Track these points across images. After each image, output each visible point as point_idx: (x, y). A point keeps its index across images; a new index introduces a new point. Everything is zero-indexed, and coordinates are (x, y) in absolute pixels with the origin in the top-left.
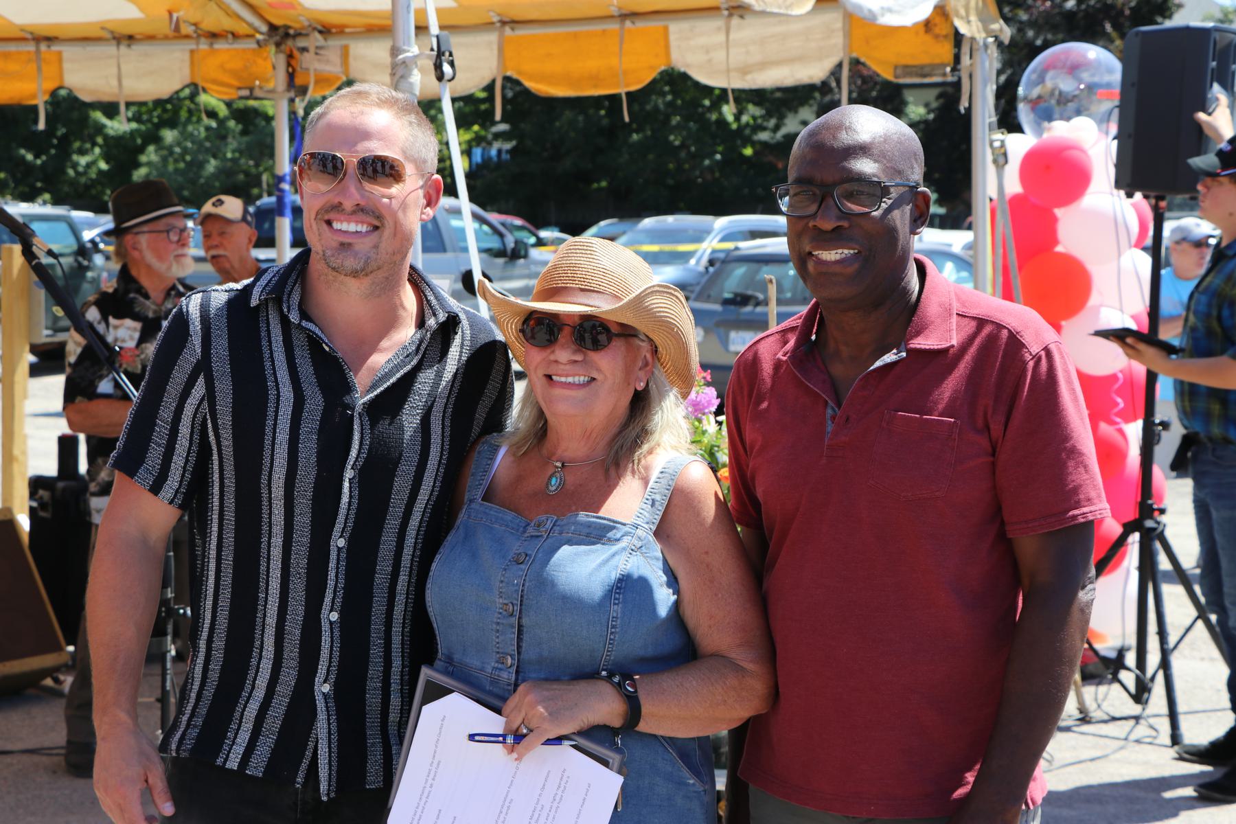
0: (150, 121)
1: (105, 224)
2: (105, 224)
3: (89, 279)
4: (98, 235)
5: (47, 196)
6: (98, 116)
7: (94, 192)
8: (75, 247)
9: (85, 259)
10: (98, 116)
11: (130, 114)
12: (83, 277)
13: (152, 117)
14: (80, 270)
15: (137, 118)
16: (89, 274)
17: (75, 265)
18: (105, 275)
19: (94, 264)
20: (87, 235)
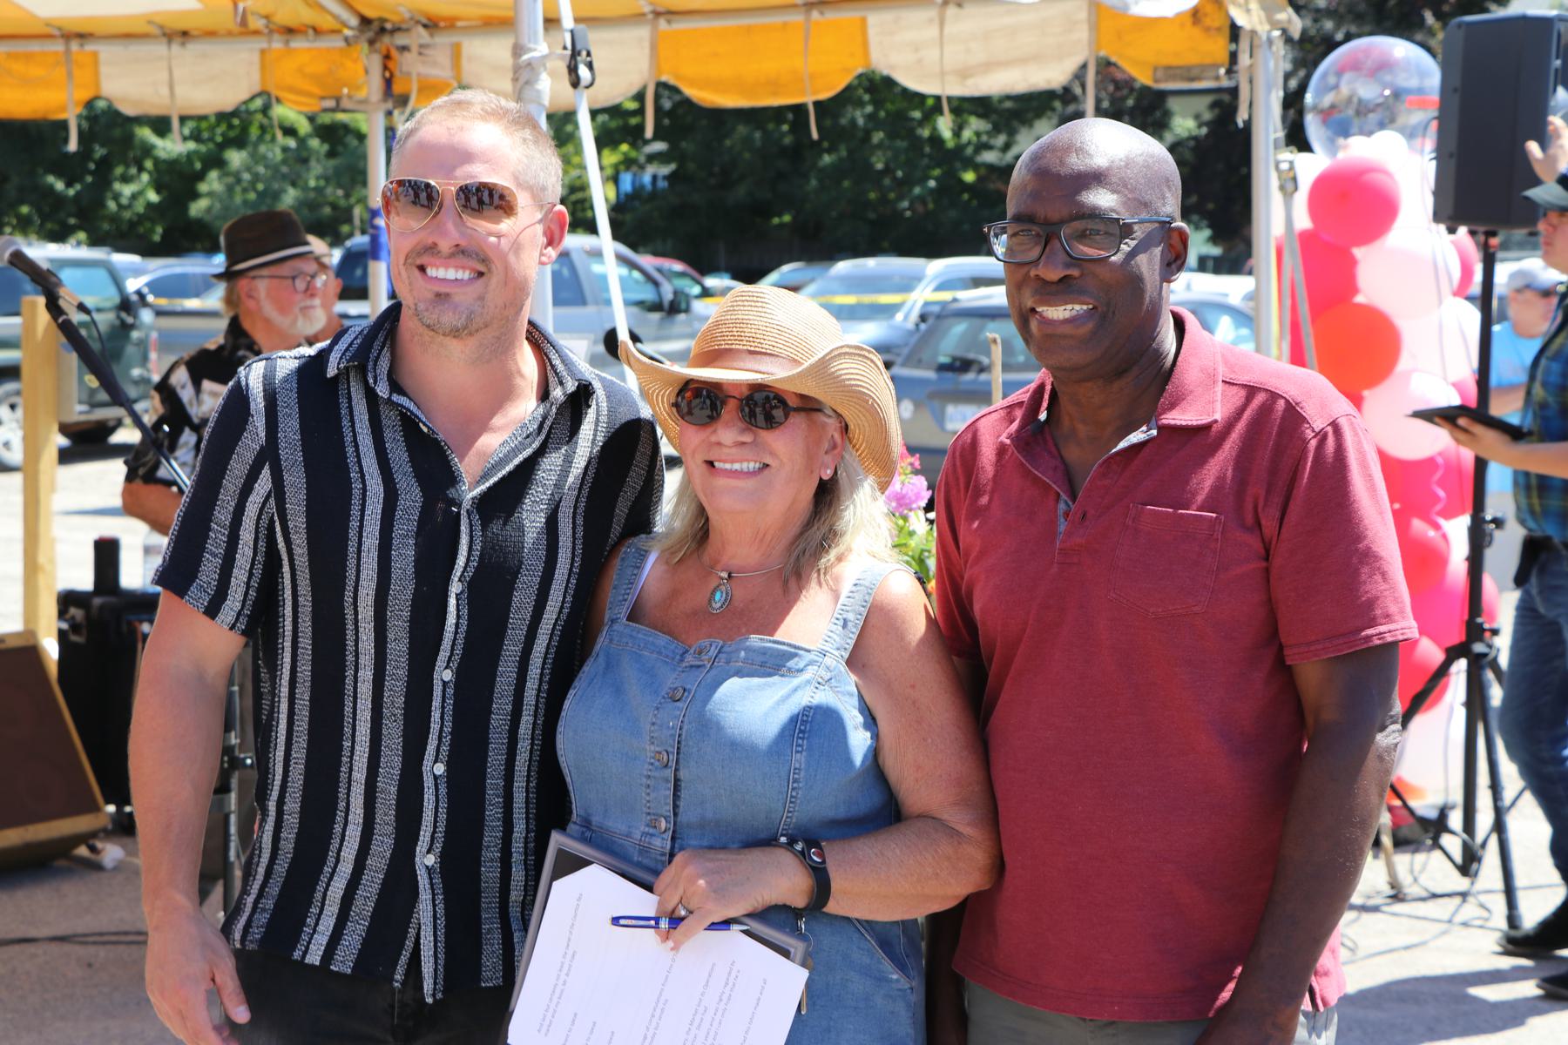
0: (211, 139)
1: (155, 270)
2: (155, 270)
3: (135, 342)
4: (148, 285)
5: (82, 235)
6: (145, 133)
7: (141, 230)
8: (117, 300)
9: (129, 314)
10: (145, 133)
11: (186, 131)
12: (127, 337)
13: (214, 135)
14: (125, 328)
15: (196, 136)
16: (135, 335)
17: (117, 322)
18: (154, 335)
19: (142, 324)
20: (132, 285)
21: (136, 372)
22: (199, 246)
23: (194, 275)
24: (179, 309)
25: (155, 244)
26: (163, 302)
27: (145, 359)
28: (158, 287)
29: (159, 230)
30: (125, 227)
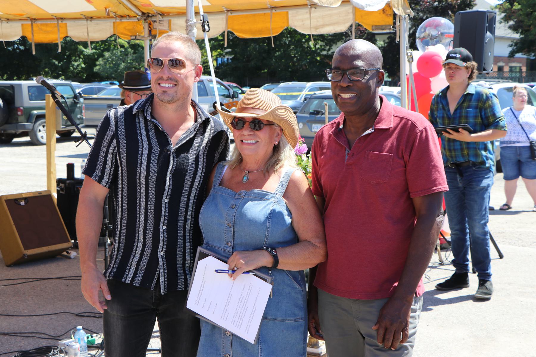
0: (100, 49)
1: (83, 87)
2: (83, 87)
3: (79, 107)
4: (81, 91)
5: (63, 77)
6: (81, 47)
7: (80, 75)
8: (73, 95)
9: (76, 100)
10: (81, 47)
11: (93, 47)
12: (76, 106)
13: (101, 48)
14: (75, 104)
15: (95, 48)
16: (78, 105)
17: (73, 102)
18: (84, 105)
19: (80, 101)
20: (77, 91)
21: (79, 116)
22: (96, 80)
23: (95, 87)
24: (91, 98)
26: (86, 96)
27: (81, 112)
28: (84, 91)
29: (85, 75)
30: (75, 74)
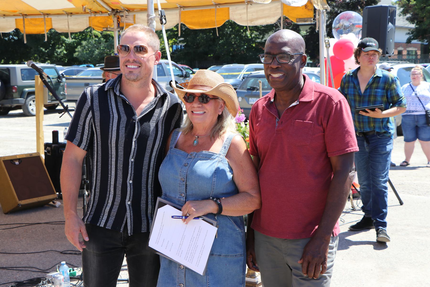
0: (78, 39)
3: (62, 85)
4: (64, 72)
5: (49, 61)
6: (63, 37)
7: (62, 60)
8: (56, 76)
9: (60, 80)
10: (63, 37)
11: (72, 37)
12: (60, 85)
14: (59, 83)
15: (75, 38)
16: (61, 84)
17: (57, 81)
18: (66, 84)
19: (63, 81)
20: (61, 73)
21: (62, 93)
22: (76, 63)
23: (75, 70)
24: (71, 78)
25: (66, 63)
27: (64, 89)
28: (66, 73)
29: (67, 60)
30: (59, 59)
